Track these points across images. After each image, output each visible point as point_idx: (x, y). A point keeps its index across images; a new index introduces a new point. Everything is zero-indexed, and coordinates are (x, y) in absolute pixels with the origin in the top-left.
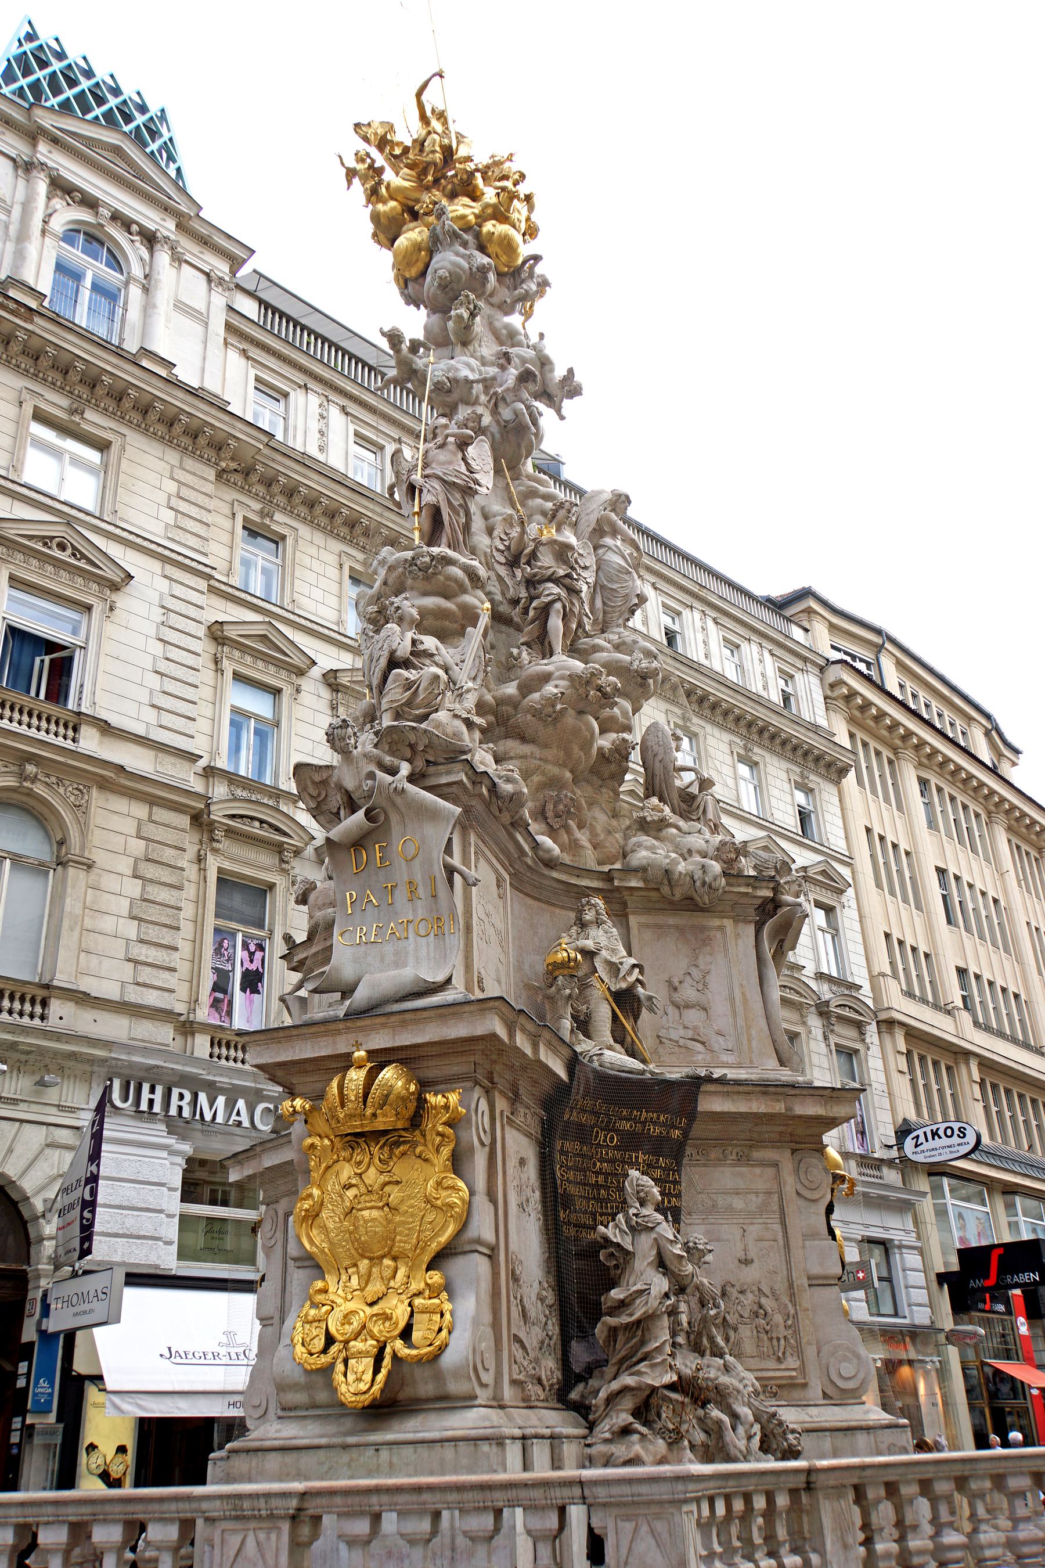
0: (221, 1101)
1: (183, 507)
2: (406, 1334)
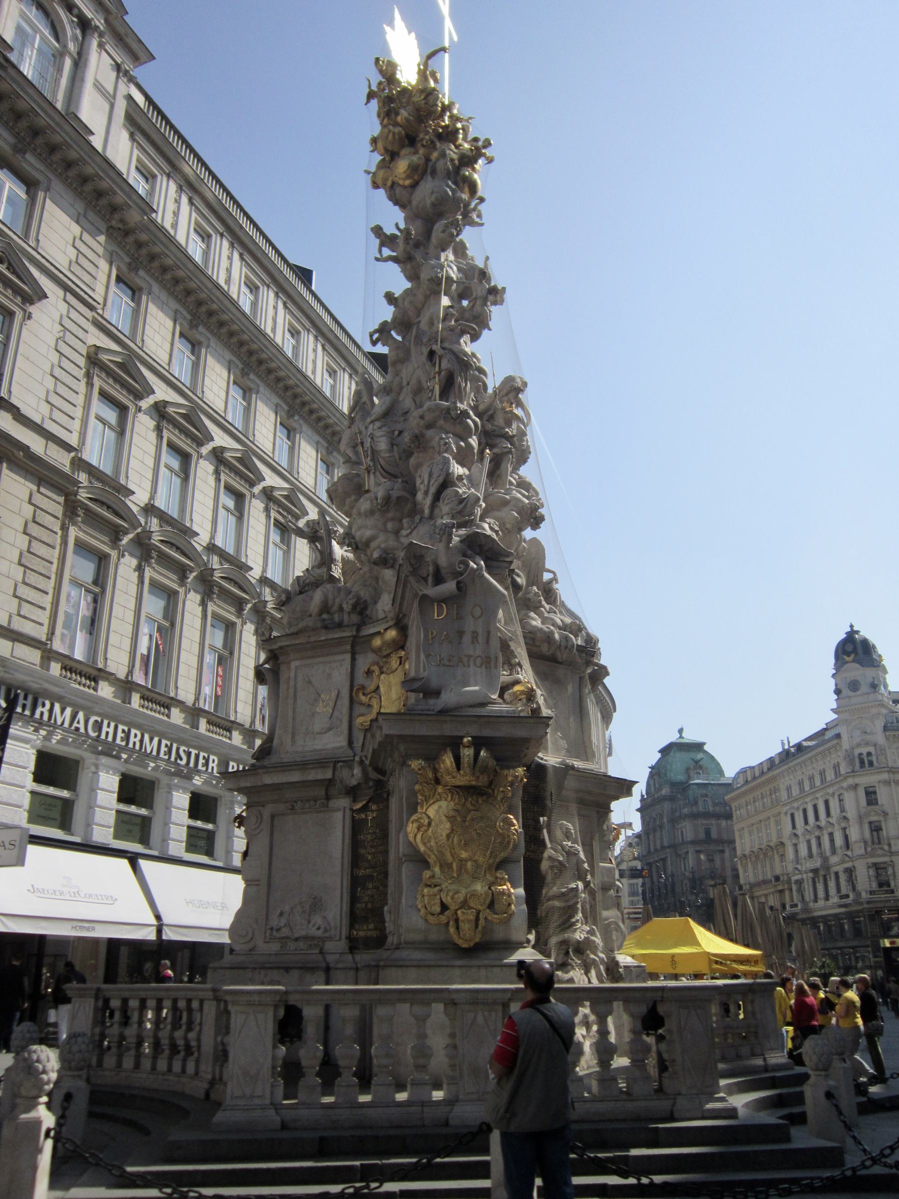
0: (68, 711)
1: (83, 248)
2: (491, 905)
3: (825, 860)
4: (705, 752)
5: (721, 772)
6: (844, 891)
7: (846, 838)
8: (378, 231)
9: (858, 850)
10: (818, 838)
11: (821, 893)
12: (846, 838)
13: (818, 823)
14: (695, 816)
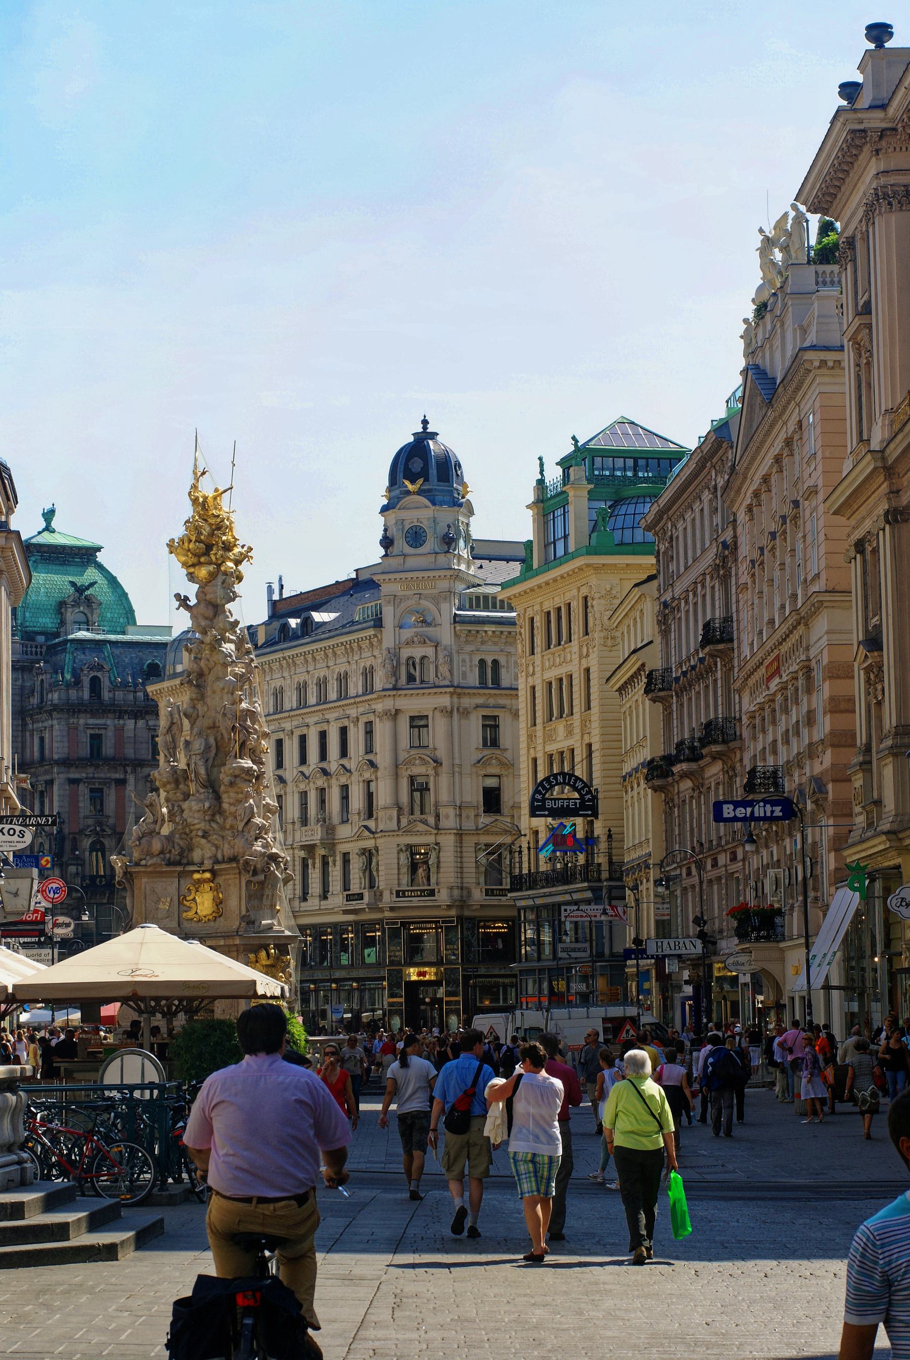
3: (330, 830)
4: (100, 567)
5: (129, 614)
6: (355, 888)
7: (370, 797)
8: (178, 596)
9: (385, 819)
10: (322, 790)
11: (315, 887)
12: (370, 797)
13: (324, 765)
14: (72, 709)
